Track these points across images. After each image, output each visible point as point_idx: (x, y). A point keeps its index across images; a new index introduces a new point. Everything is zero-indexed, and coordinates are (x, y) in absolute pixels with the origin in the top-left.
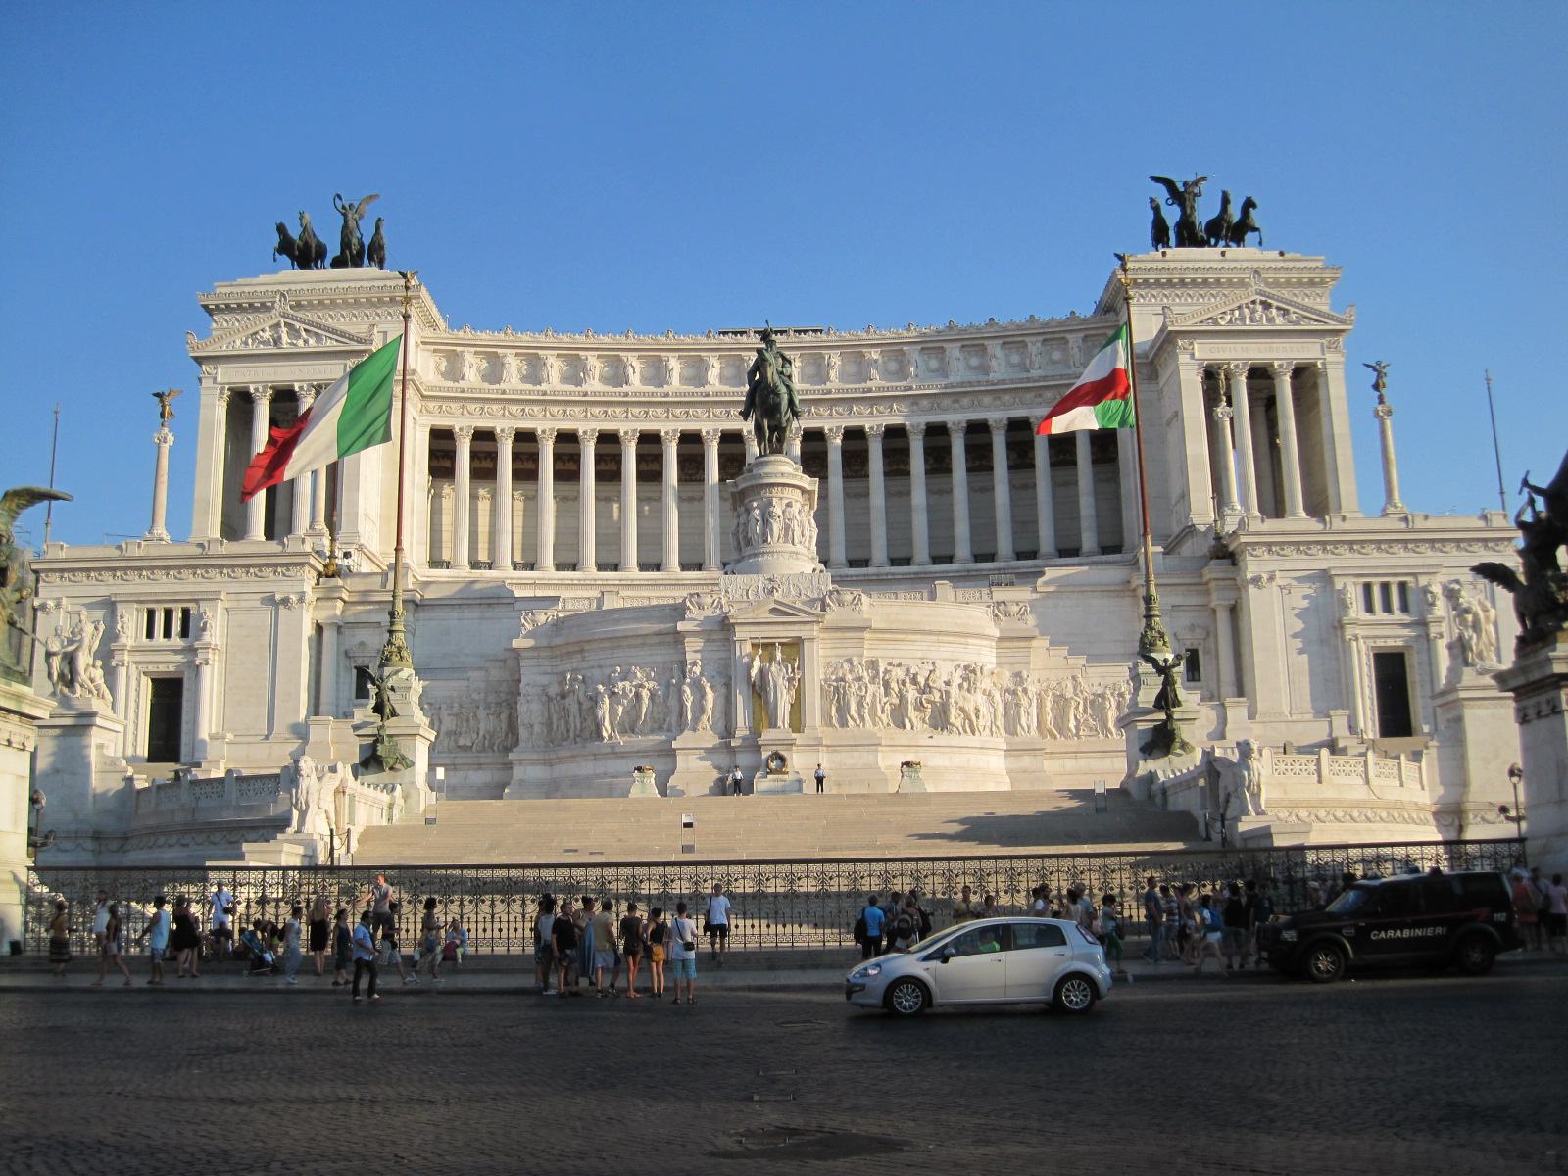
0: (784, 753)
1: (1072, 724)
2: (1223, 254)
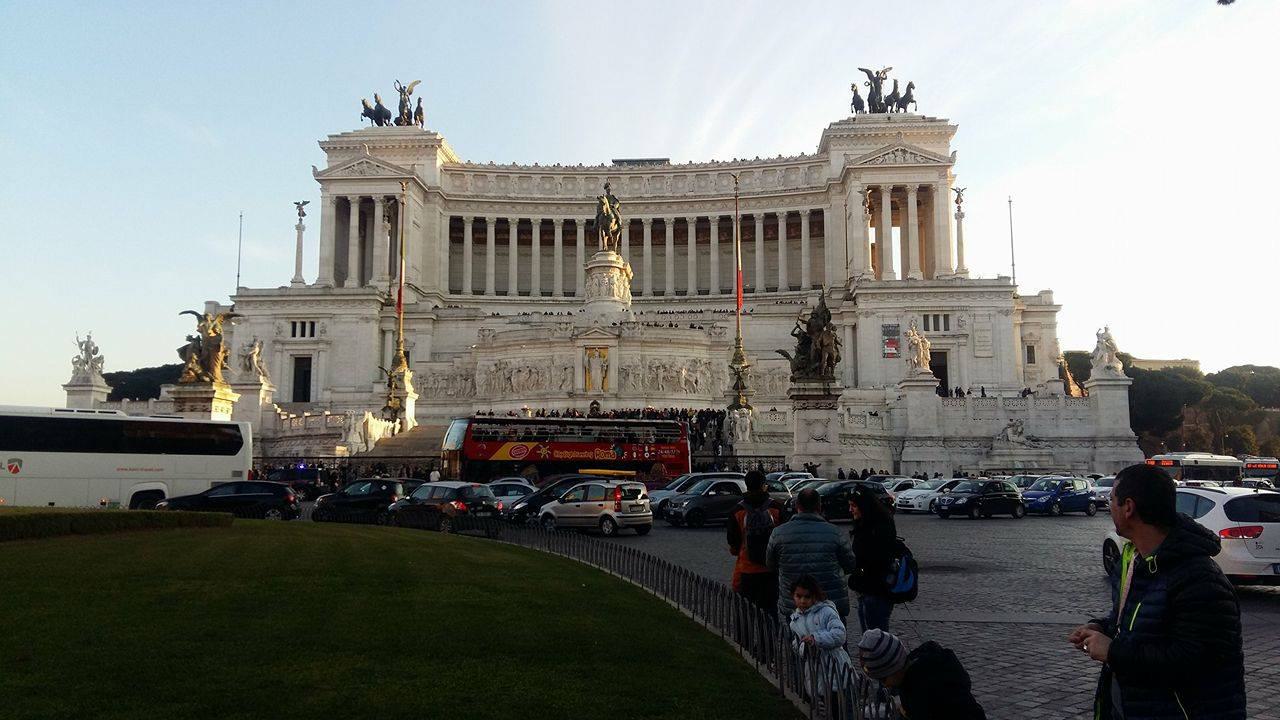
2: (889, 118)
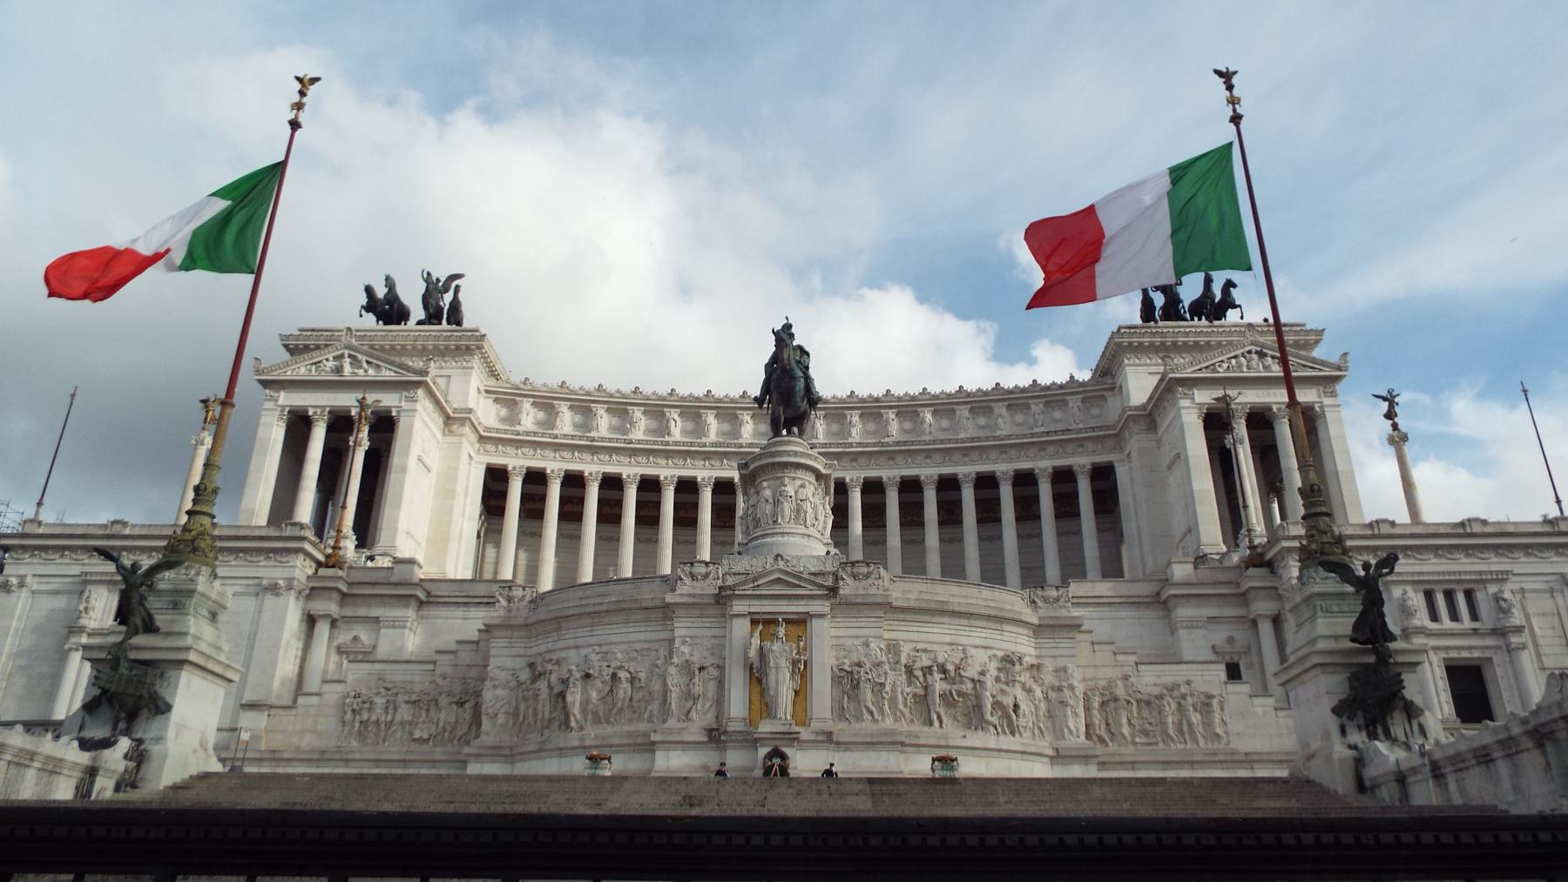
0: (788, 751)
1: (1126, 730)
